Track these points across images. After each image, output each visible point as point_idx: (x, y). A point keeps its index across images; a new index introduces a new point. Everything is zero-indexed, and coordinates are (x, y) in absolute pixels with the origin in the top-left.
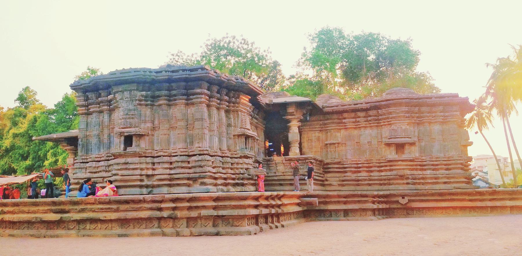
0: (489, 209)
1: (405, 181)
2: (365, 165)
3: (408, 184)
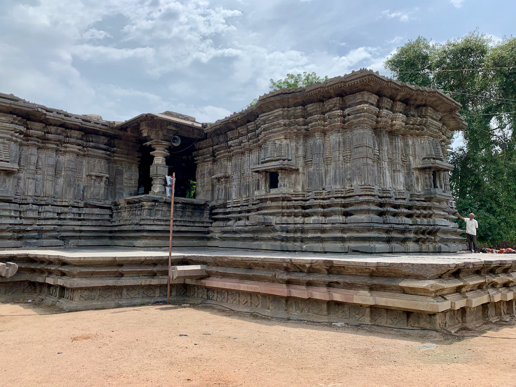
0: (325, 306)
1: (269, 236)
3: (274, 239)
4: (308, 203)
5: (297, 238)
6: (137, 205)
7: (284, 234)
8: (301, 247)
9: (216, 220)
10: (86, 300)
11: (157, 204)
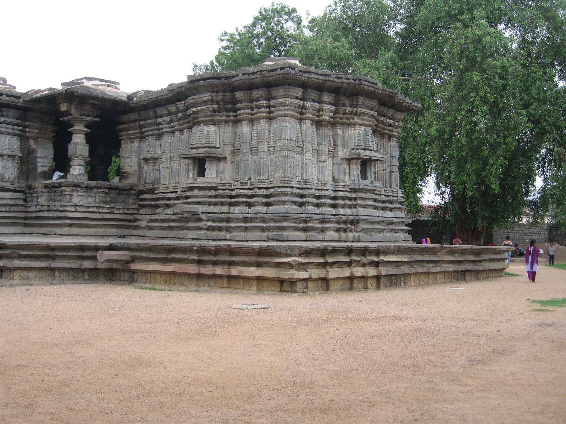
2: (174, 195)
3: (200, 228)
4: (233, 193)
5: (222, 227)
6: (56, 189)
7: (210, 224)
8: (225, 236)
9: (143, 206)
10: (24, 279)
11: (78, 189)
